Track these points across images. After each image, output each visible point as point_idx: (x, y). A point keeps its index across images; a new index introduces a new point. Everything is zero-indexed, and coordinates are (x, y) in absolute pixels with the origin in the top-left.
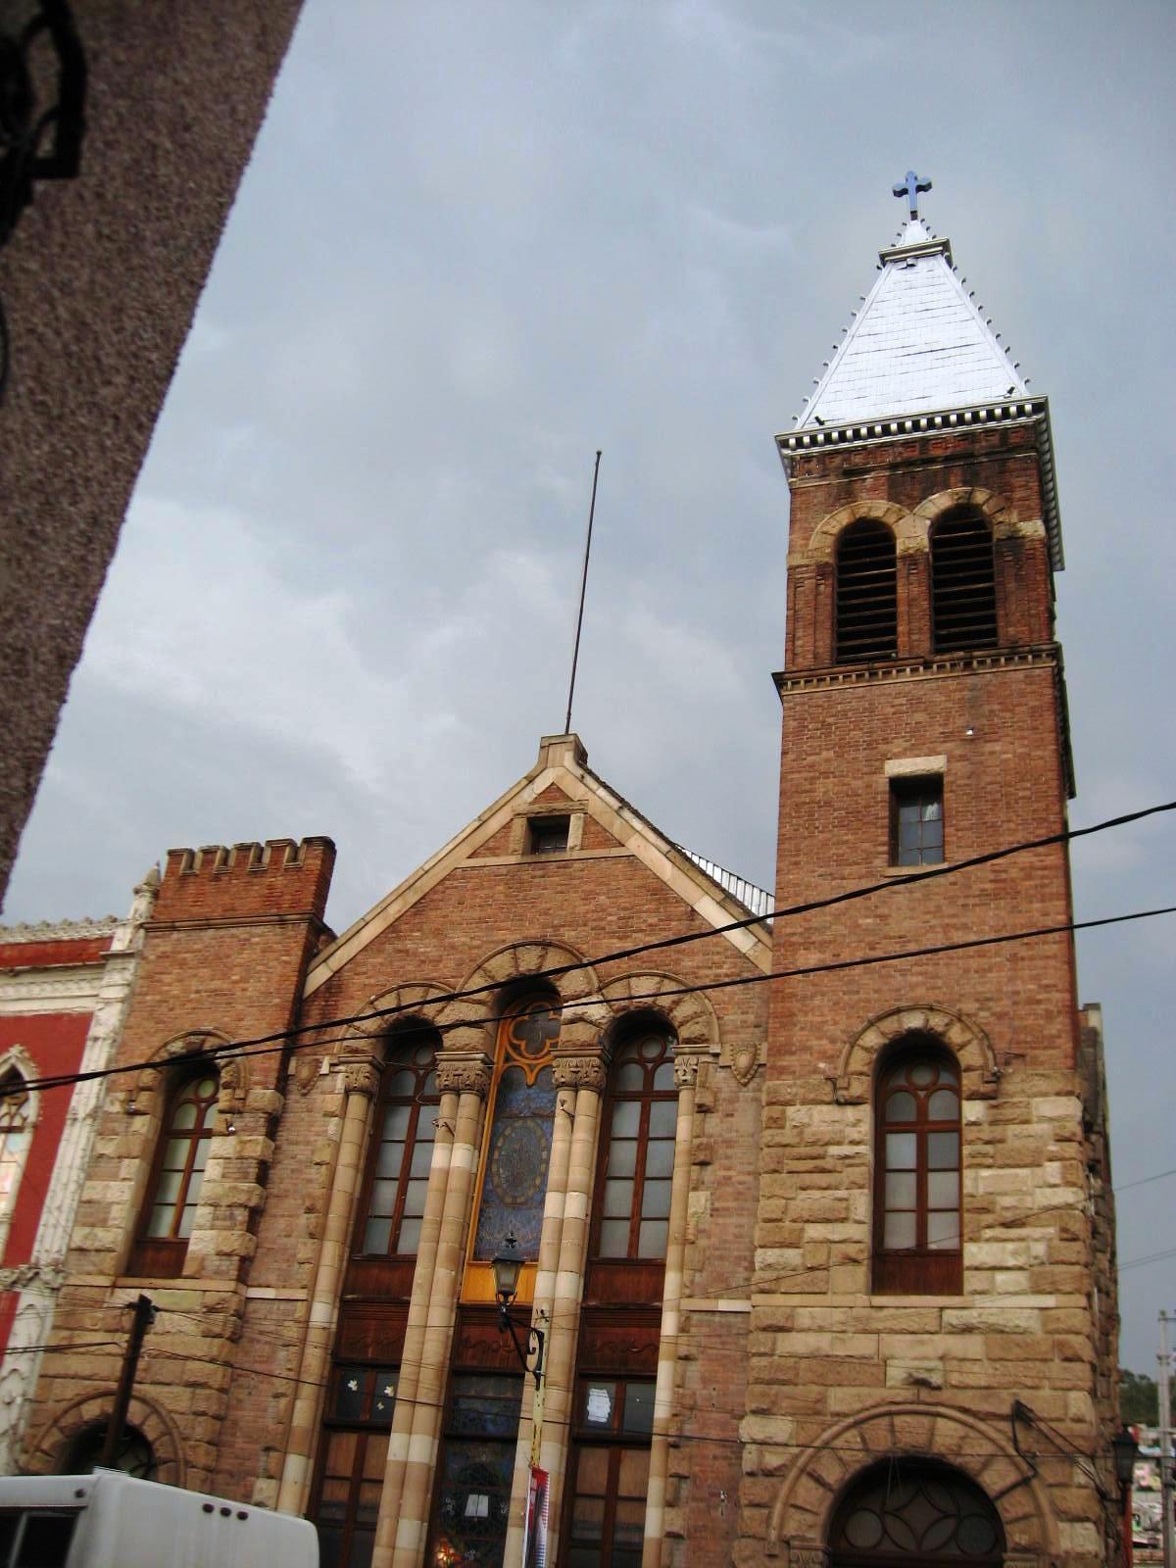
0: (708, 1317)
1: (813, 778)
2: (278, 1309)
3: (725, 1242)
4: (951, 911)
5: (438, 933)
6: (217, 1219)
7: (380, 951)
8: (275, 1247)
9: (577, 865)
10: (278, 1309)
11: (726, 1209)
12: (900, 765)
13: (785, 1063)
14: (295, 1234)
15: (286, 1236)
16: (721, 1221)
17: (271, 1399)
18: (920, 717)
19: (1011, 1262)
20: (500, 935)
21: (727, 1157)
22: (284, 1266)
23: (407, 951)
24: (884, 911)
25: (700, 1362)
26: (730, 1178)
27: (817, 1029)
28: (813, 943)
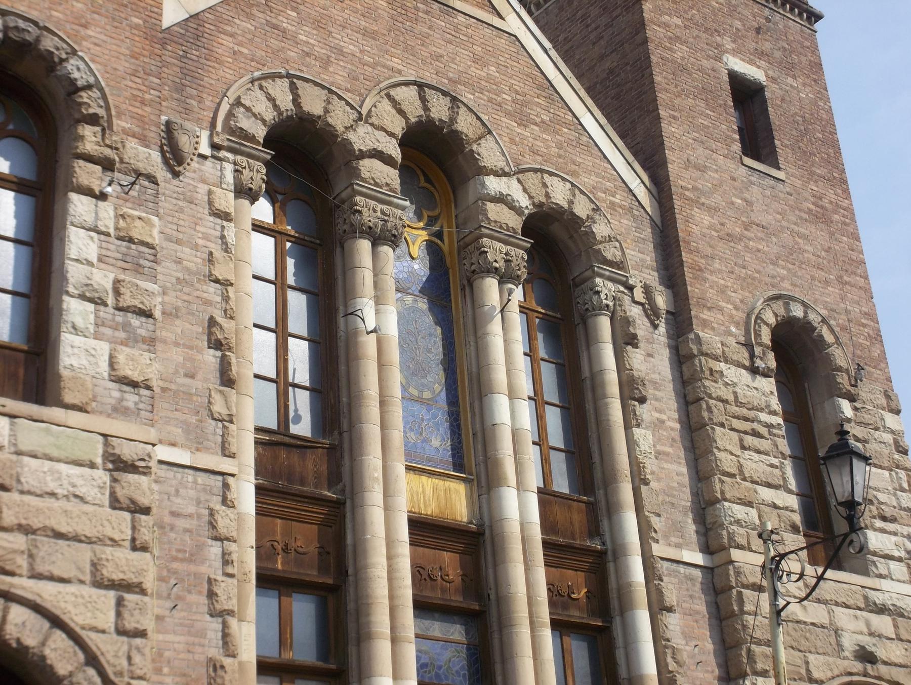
0: (674, 566)
1: (671, 38)
2: (195, 482)
3: (673, 488)
4: (793, 219)
5: (318, 24)
6: (103, 325)
7: (250, 16)
8: (173, 387)
9: (461, 18)
10: (195, 482)
11: (667, 454)
12: (736, 64)
13: (705, 317)
14: (200, 376)
15: (186, 375)
16: (665, 465)
17: (208, 617)
18: (738, 24)
19: (896, 554)
20: (396, 63)
21: (656, 399)
22: (193, 419)
23: (284, 31)
24: (747, 195)
25: (677, 615)
26: (663, 422)
27: (722, 291)
28: (703, 204)
